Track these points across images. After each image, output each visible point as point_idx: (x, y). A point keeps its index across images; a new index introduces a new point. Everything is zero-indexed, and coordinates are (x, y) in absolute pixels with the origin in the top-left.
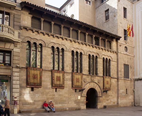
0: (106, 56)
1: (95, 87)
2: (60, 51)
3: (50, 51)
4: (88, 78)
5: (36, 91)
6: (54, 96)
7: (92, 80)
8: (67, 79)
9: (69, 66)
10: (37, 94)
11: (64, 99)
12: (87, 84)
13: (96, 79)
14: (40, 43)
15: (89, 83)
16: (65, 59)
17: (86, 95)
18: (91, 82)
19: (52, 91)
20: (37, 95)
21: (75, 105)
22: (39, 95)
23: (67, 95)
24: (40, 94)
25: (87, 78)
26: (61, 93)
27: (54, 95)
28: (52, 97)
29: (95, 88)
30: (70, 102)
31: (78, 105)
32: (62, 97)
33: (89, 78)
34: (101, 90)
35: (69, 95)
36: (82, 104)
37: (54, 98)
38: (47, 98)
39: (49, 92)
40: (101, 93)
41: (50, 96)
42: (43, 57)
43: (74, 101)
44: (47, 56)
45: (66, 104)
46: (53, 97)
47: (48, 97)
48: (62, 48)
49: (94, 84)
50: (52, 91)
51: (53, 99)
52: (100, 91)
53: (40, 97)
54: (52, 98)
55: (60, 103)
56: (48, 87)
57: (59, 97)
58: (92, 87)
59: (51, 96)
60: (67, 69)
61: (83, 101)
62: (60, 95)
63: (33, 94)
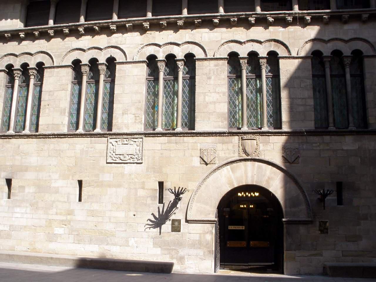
0: (330, 45)
1: (268, 182)
2: (100, 67)
3: (68, 74)
4: (225, 146)
5: (16, 198)
6: (69, 215)
7: (248, 150)
8: (122, 157)
9: (133, 110)
10: (19, 206)
11: (109, 227)
12: (218, 168)
13: (269, 147)
14: (38, 61)
15: (228, 167)
16: (117, 91)
17: (214, 216)
18: (240, 160)
19: (66, 200)
20: (18, 210)
21: (158, 251)
22: (23, 210)
23: (121, 215)
24: (27, 207)
25: (219, 146)
26: (95, 206)
27: (70, 213)
28: (64, 218)
29: (264, 185)
30: (132, 242)
31: (173, 253)
32: (100, 219)
33: (230, 146)
34: (303, 192)
35: (132, 214)
36: (193, 252)
37: (70, 222)
38: (46, 221)
39: (54, 202)
40: (303, 207)
41: (57, 214)
42: (44, 96)
43: (153, 238)
44: (56, 94)
45: (115, 244)
46: (69, 217)
47: (50, 217)
48: (109, 56)
49: (259, 167)
50: (66, 200)
51: (69, 226)
52: (301, 197)
53: (25, 216)
54: (62, 221)
55: (91, 241)
56: (54, 185)
57: (90, 219)
58: (250, 183)
59: (61, 214)
60: (126, 121)
61: (197, 237)
62: (92, 213)
63: (9, 207)
